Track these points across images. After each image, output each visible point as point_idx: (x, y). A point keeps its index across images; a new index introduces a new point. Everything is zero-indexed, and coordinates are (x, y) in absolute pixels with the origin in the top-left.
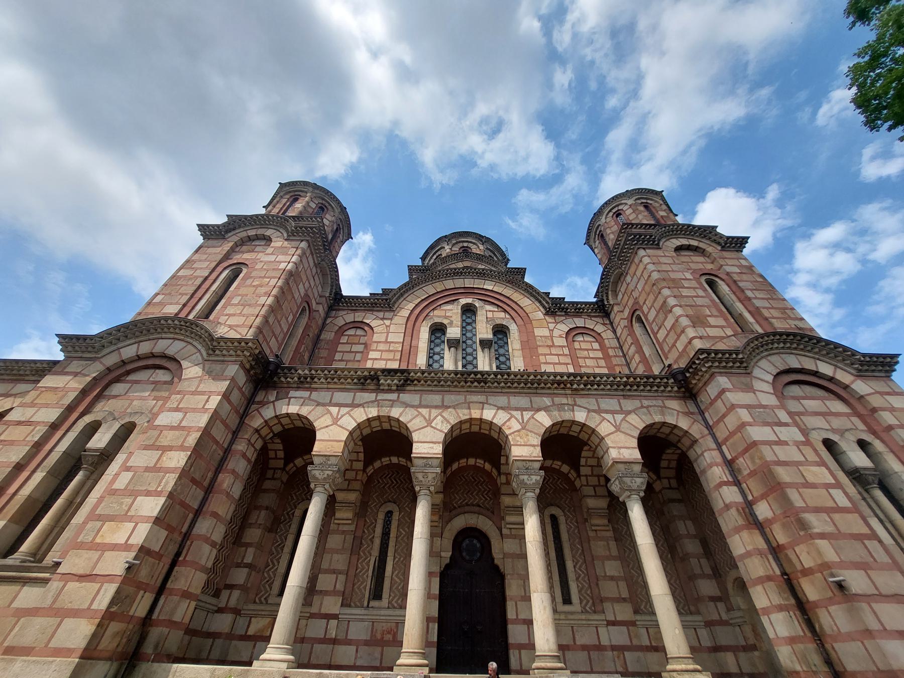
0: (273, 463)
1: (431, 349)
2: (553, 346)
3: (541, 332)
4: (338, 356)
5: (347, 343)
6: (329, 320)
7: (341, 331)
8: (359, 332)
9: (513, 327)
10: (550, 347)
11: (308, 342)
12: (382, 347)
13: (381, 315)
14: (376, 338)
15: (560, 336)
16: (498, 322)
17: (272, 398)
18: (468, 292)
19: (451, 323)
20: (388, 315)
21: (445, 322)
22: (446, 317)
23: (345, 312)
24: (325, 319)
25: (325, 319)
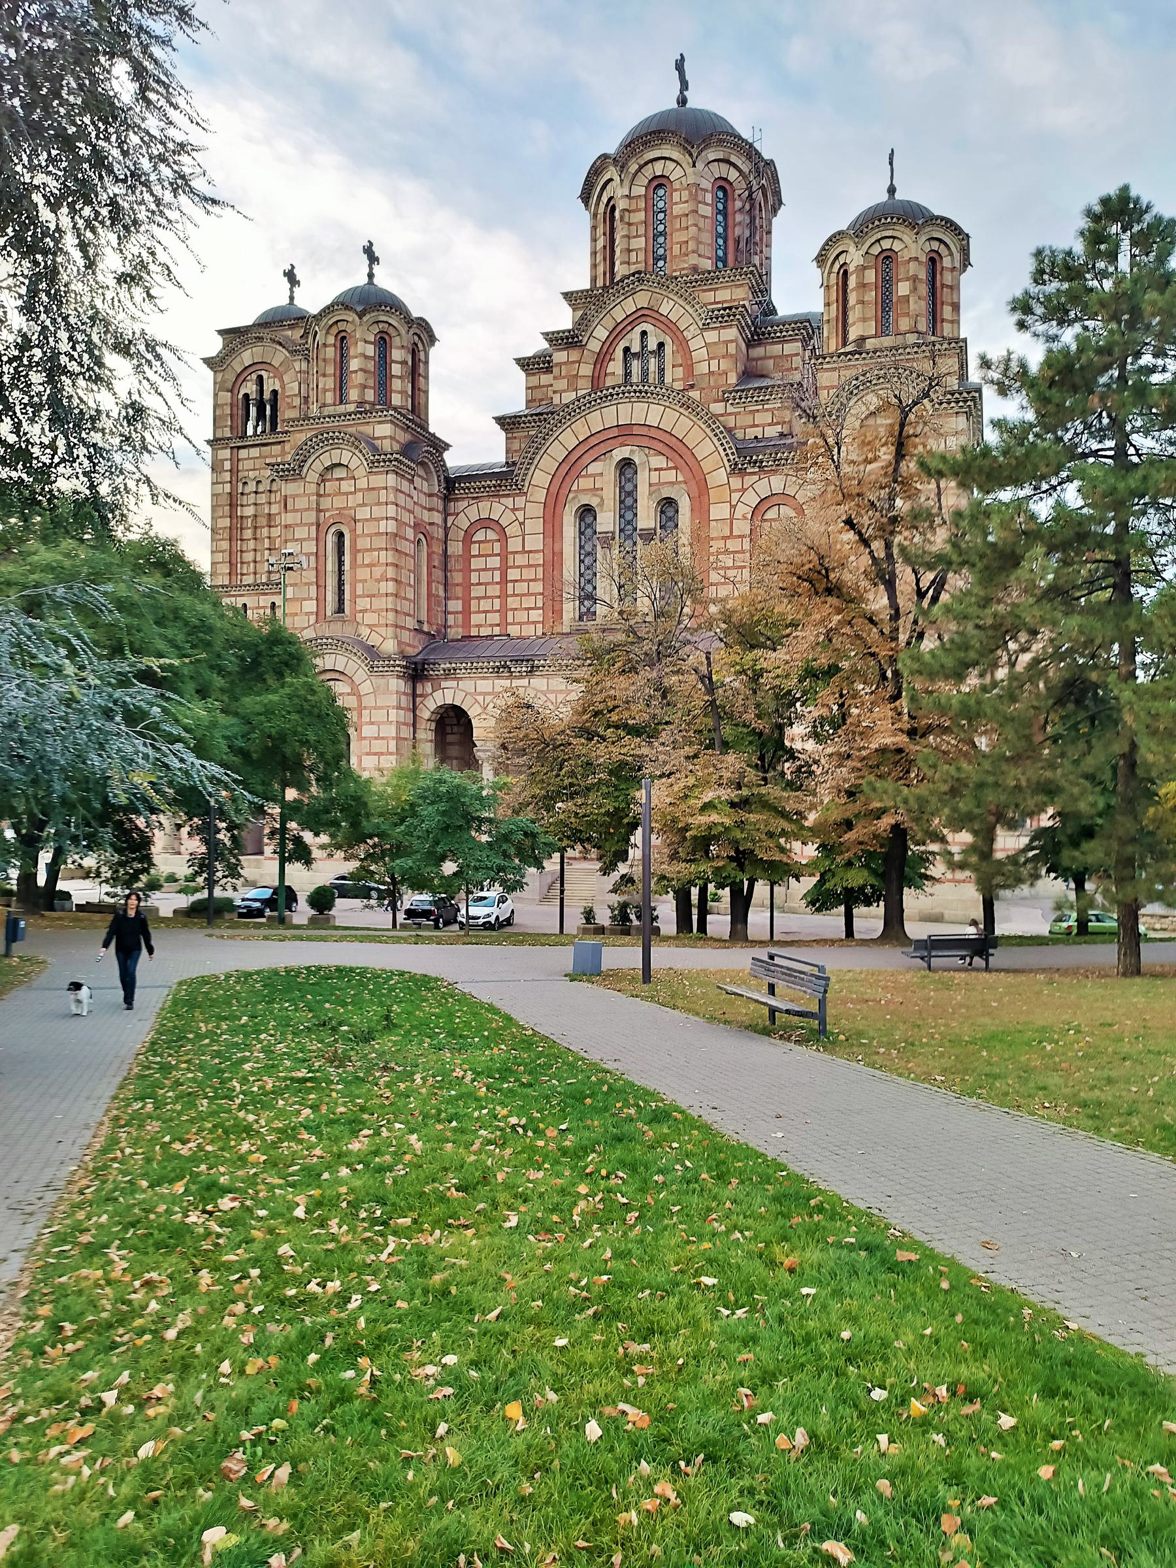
0: (448, 721)
1: (581, 547)
2: (731, 536)
3: (719, 512)
4: (474, 578)
5: (479, 556)
6: (450, 519)
7: (468, 539)
8: (492, 535)
9: (684, 504)
10: (725, 538)
11: (438, 574)
12: (521, 560)
13: (509, 502)
14: (514, 545)
15: (745, 518)
16: (666, 493)
17: (429, 690)
18: (625, 432)
19: (602, 504)
20: (520, 501)
21: (594, 502)
22: (595, 490)
23: (465, 503)
24: (445, 521)
25: (445, 521)
